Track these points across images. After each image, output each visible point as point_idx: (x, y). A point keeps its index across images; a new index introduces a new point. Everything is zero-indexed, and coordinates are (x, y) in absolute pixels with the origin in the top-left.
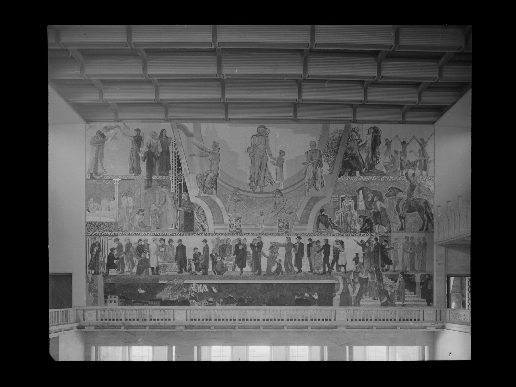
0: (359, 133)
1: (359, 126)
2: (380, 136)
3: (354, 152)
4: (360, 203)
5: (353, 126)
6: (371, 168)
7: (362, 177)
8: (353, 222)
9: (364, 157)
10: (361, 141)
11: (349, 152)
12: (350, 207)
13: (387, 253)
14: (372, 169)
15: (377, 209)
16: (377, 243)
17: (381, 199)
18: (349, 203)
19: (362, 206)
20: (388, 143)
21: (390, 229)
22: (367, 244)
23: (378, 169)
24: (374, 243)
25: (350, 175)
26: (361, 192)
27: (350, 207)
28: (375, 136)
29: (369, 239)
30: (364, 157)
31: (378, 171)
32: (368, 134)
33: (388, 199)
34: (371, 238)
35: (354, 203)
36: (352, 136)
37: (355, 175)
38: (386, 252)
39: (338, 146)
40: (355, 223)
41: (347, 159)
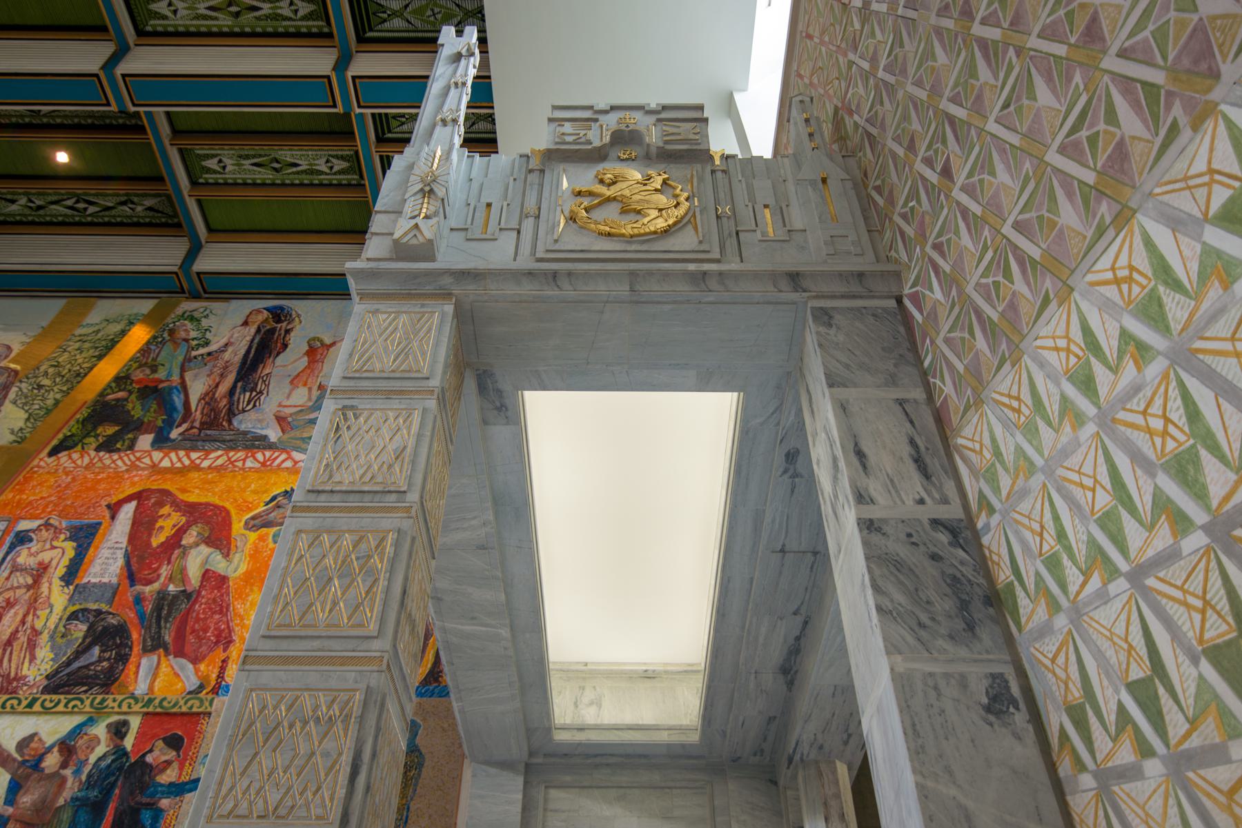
0: (205, 323)
1: (217, 306)
2: (288, 332)
3: (161, 374)
4: (105, 552)
5: (187, 306)
6: (216, 425)
7: (157, 455)
8: (23, 638)
9: (197, 388)
10: (207, 344)
11: (138, 375)
12: (43, 568)
13: (158, 813)
14: (219, 426)
15: (184, 577)
16: (120, 753)
17: (220, 538)
18: (46, 556)
19: (106, 565)
20: (317, 352)
21: (221, 676)
22: (52, 761)
23: (243, 427)
24: (100, 750)
25: (108, 446)
26: (128, 510)
27: (43, 568)
28: (272, 331)
29: (77, 731)
30: (197, 388)
31: (245, 433)
32: (246, 323)
33: (253, 536)
34: (91, 721)
35: (70, 553)
36: (172, 332)
37: (131, 447)
38: (152, 806)
39: (100, 357)
40: (32, 646)
41: (121, 394)
